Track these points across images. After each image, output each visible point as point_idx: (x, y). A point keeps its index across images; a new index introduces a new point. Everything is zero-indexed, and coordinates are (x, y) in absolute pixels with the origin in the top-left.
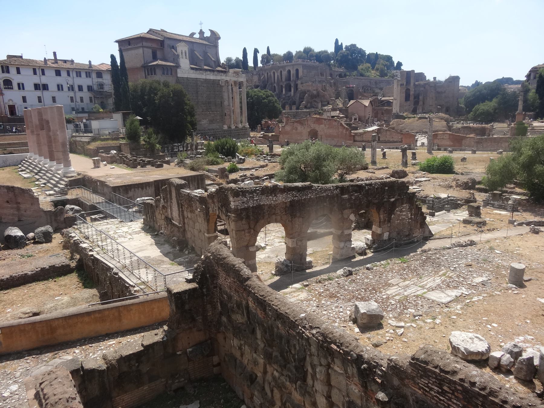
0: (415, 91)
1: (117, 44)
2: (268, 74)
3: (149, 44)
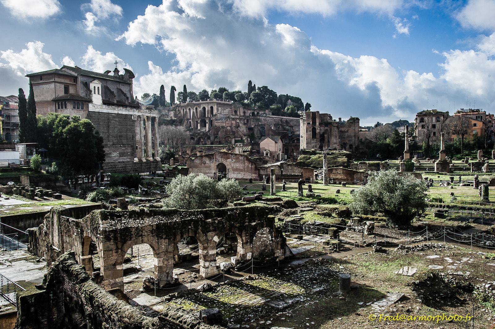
1: (28, 78)
3: (62, 80)
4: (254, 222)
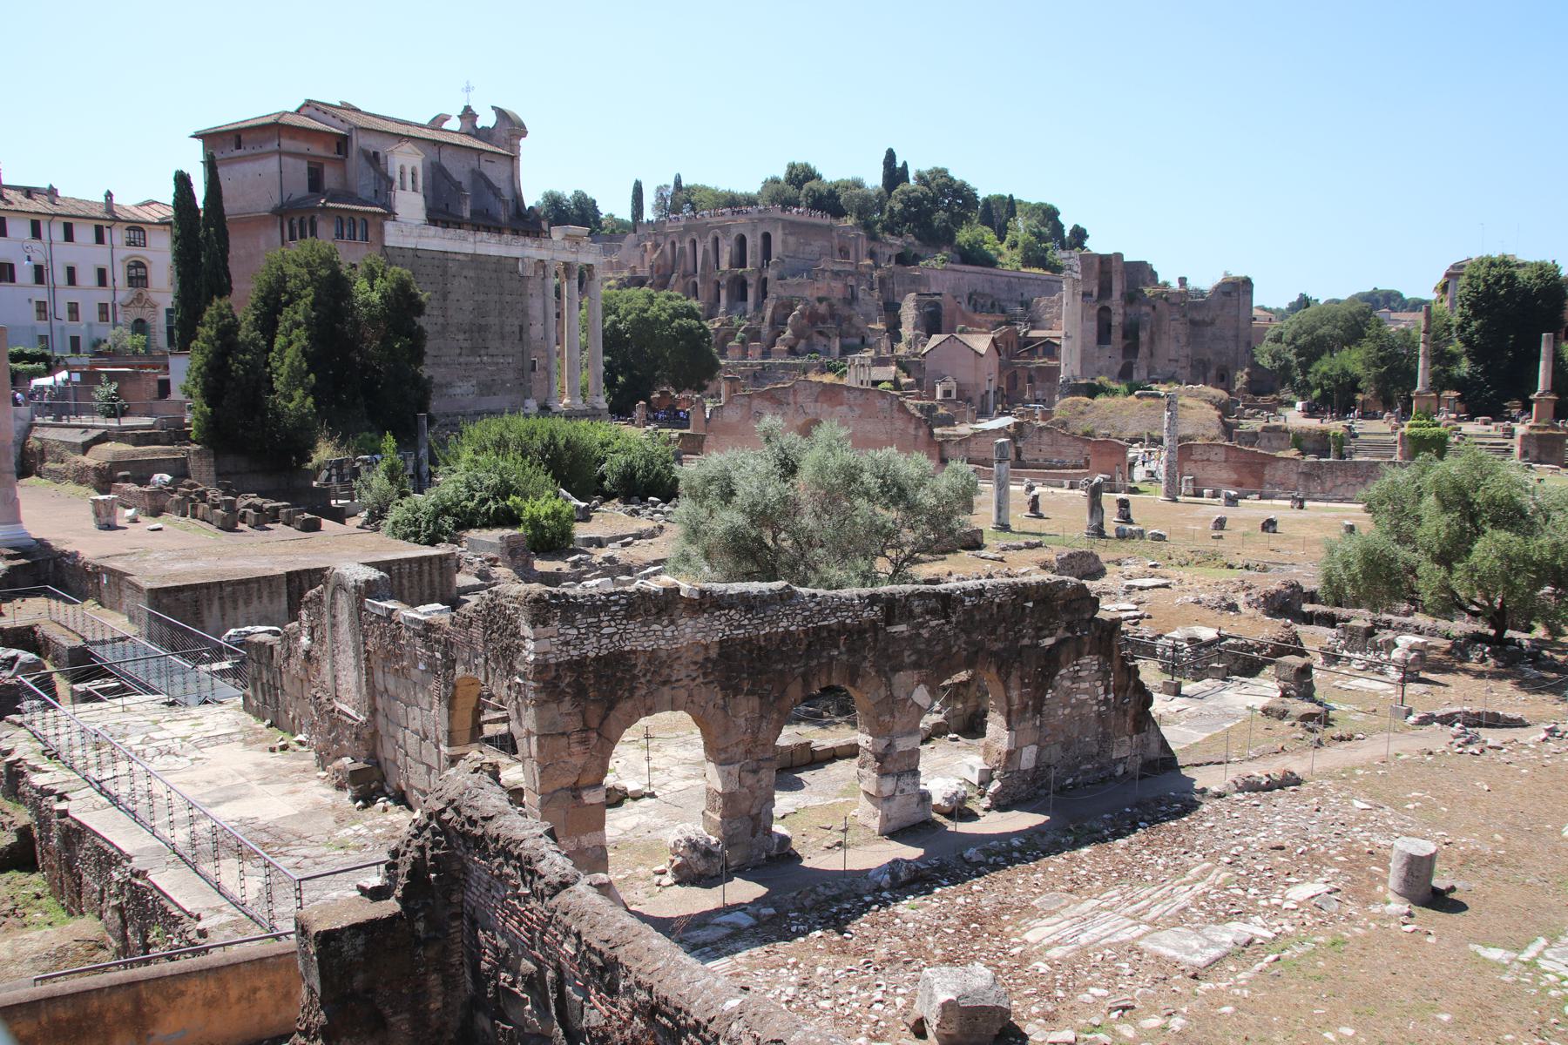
0: (1125, 314)
1: (199, 143)
2: (673, 244)
3: (301, 146)
4: (1051, 635)
